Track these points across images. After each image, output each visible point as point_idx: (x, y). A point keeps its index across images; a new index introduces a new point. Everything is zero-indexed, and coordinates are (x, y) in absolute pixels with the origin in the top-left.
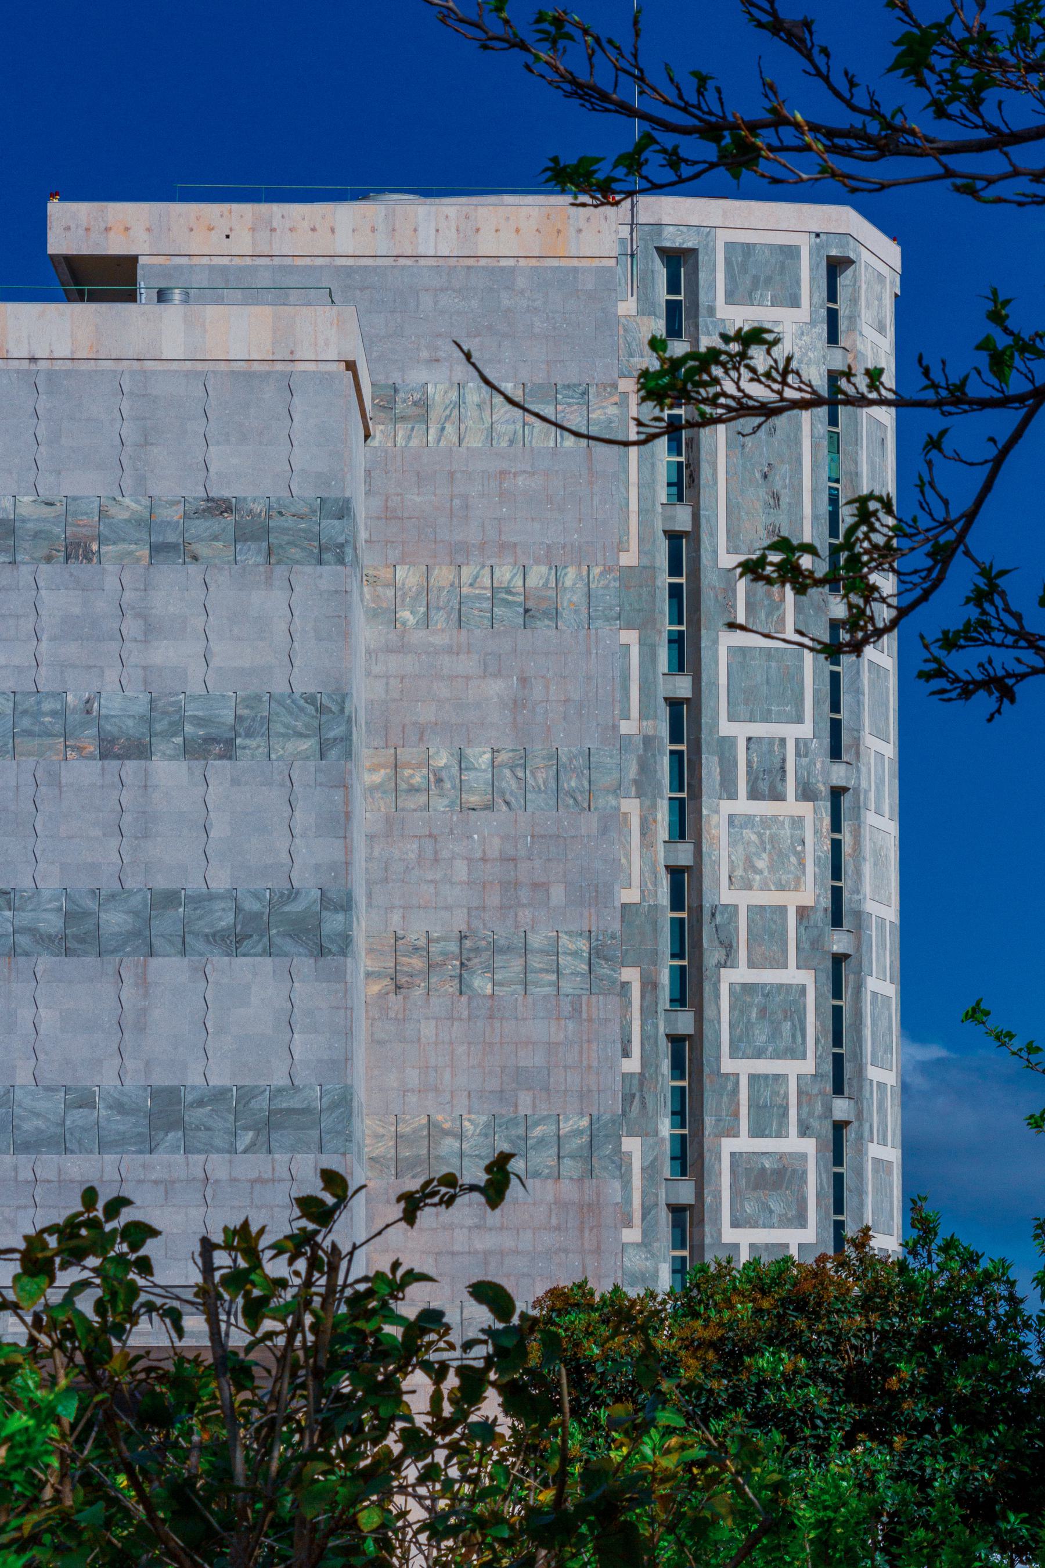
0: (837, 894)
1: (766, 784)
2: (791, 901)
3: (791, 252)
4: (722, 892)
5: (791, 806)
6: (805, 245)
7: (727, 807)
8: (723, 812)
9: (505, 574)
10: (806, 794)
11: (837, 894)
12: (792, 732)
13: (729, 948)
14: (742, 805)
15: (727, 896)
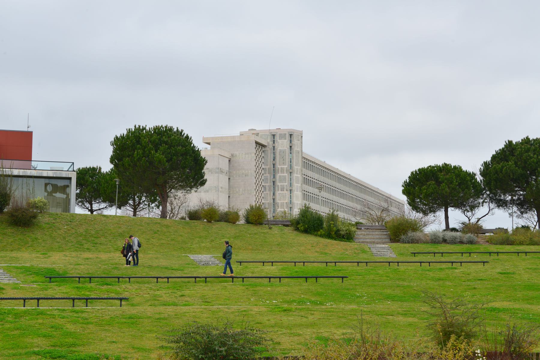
0: (291, 201)
1: (282, 190)
2: (285, 202)
3: (286, 134)
4: (277, 201)
5: (285, 192)
6: (287, 133)
7: (278, 192)
8: (278, 193)
9: (244, 172)
10: (287, 190)
11: (291, 201)
12: (285, 184)
13: (278, 207)
14: (280, 192)
15: (278, 201)
